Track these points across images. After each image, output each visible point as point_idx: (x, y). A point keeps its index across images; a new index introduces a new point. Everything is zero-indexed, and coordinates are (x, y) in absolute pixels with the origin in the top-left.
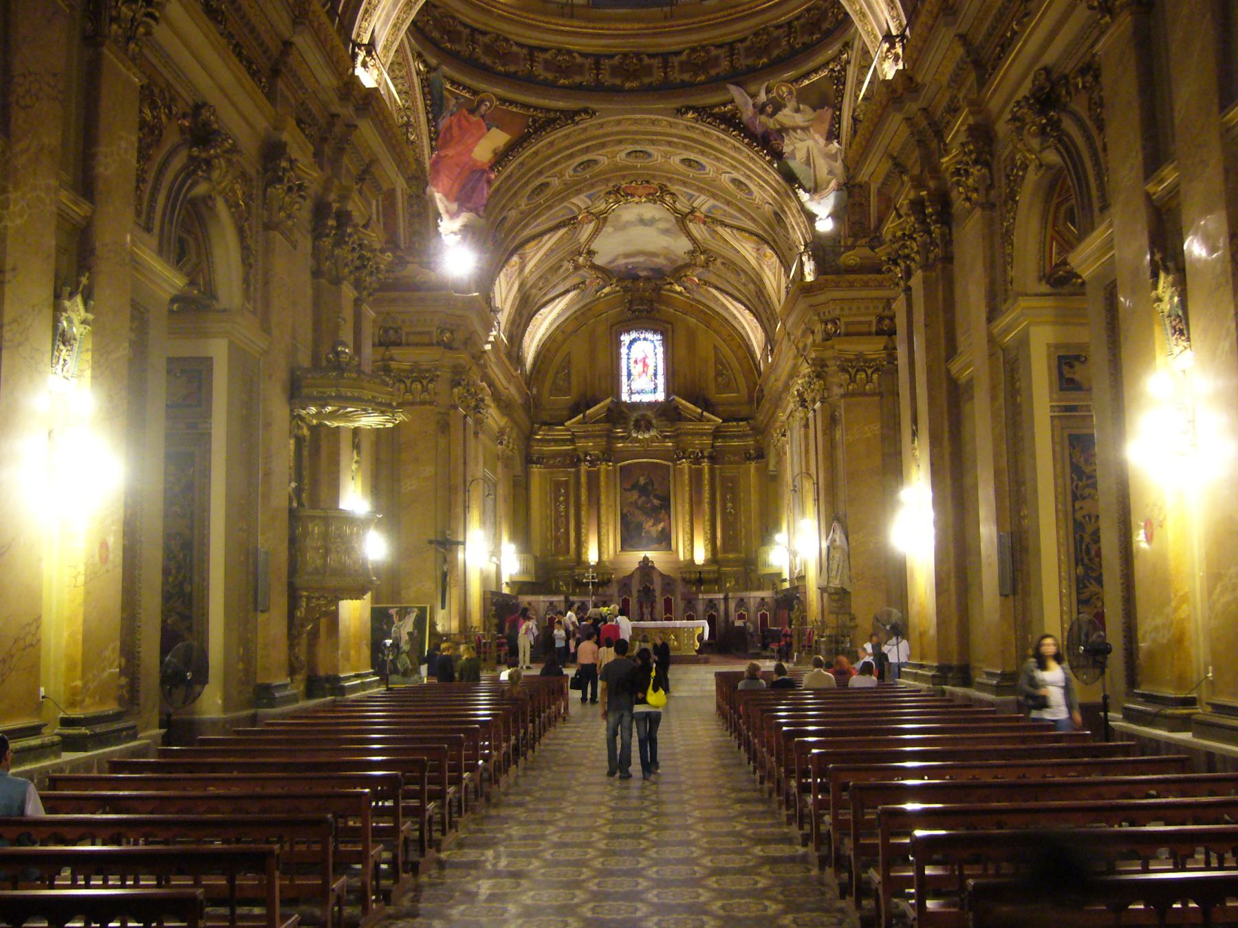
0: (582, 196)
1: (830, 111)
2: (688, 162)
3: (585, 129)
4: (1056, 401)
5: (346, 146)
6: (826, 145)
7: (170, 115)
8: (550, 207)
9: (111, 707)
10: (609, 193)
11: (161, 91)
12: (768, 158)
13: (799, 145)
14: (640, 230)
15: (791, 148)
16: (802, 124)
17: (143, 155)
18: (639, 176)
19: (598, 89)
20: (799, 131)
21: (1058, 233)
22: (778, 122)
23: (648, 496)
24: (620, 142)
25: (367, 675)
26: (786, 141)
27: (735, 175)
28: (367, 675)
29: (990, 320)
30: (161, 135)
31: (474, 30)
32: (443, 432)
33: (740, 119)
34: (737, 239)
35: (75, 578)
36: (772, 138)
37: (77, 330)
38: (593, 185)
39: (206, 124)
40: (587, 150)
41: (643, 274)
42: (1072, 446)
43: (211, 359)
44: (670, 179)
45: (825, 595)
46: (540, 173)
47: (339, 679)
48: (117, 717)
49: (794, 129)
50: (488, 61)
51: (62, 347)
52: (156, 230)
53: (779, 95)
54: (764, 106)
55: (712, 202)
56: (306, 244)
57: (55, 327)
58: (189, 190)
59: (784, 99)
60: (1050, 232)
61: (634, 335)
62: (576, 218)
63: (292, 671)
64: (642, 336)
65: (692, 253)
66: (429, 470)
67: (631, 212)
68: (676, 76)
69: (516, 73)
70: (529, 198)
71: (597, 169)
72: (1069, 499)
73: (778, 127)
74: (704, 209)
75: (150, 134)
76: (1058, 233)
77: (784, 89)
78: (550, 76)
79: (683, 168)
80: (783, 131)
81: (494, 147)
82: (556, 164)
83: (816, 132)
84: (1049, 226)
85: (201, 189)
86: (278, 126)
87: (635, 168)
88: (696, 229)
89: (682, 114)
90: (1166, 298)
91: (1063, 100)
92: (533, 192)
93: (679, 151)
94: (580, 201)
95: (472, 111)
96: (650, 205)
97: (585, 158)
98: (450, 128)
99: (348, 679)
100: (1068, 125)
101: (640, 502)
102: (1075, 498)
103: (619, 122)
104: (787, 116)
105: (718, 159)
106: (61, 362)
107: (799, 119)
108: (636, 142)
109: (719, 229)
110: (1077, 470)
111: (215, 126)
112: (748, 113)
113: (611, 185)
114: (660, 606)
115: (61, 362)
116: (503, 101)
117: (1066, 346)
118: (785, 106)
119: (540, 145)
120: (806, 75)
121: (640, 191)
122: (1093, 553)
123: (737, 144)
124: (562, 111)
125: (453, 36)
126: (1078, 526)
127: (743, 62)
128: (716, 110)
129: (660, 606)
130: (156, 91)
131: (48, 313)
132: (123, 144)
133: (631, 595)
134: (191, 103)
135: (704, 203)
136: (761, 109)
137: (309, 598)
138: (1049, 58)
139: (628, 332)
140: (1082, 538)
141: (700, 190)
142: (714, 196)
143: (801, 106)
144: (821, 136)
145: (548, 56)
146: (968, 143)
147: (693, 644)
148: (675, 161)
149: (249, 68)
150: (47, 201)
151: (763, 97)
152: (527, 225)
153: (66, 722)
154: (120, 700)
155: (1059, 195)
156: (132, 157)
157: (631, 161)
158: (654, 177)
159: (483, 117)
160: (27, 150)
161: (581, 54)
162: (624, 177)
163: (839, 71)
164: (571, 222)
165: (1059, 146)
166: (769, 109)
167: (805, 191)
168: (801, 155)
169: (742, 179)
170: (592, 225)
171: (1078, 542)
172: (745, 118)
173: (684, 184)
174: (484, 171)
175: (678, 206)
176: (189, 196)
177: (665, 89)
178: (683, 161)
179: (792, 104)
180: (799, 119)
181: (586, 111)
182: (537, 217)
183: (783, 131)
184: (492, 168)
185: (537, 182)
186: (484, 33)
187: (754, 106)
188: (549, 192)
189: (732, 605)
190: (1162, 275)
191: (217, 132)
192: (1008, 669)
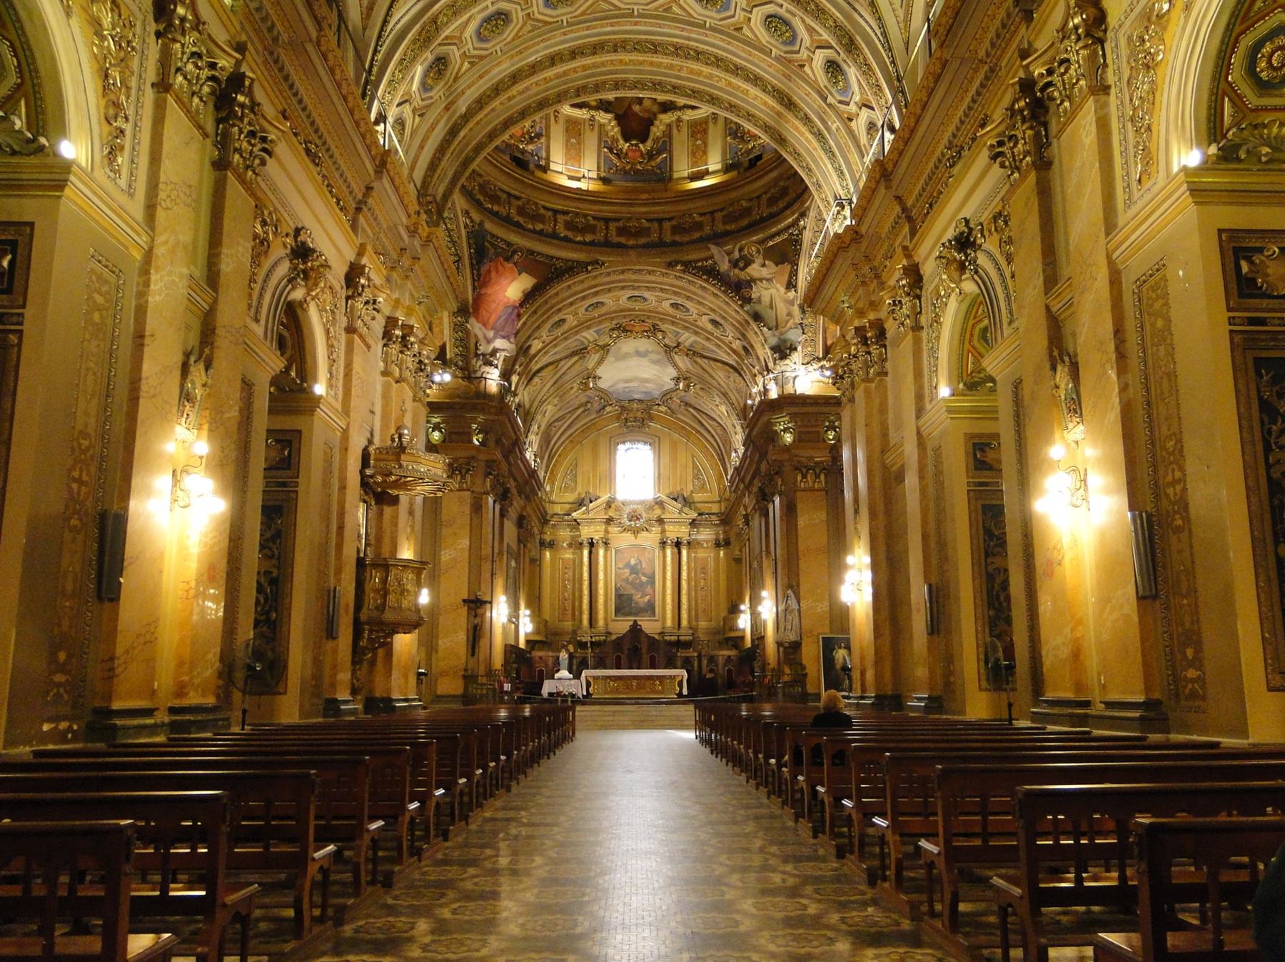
0: (591, 331)
1: (789, 266)
2: (675, 306)
3: (596, 277)
4: (972, 477)
5: (411, 274)
6: (786, 293)
7: (275, 234)
8: (566, 339)
9: (210, 700)
10: (613, 329)
11: (270, 213)
12: (739, 303)
14: (634, 362)
17: (256, 259)
18: (637, 316)
19: (607, 244)
21: (973, 347)
22: (749, 275)
23: (637, 574)
24: (623, 288)
25: (414, 700)
27: (713, 316)
28: (414, 700)
29: (918, 417)
30: (269, 247)
31: (509, 195)
32: (476, 513)
33: (718, 271)
34: (713, 369)
35: (187, 591)
37: (198, 392)
38: (600, 323)
39: (303, 243)
40: (596, 293)
41: (637, 396)
42: (984, 513)
43: (300, 432)
44: (661, 320)
45: (781, 649)
46: (560, 310)
47: (391, 700)
48: (214, 709)
49: (761, 280)
50: (521, 220)
51: (186, 403)
52: (263, 322)
55: (693, 338)
56: (378, 347)
57: (182, 386)
58: (289, 293)
60: (967, 346)
61: (628, 445)
62: (586, 348)
63: (354, 692)
64: (635, 446)
65: (677, 380)
66: (465, 543)
67: (628, 345)
68: (668, 238)
69: (542, 230)
70: (549, 331)
71: (603, 310)
72: (983, 556)
74: (687, 344)
75: (261, 246)
76: (973, 347)
78: (570, 234)
79: (671, 311)
80: (750, 282)
81: (523, 288)
82: (571, 304)
84: (967, 342)
85: (298, 294)
86: (360, 254)
87: (634, 310)
88: (683, 362)
89: (673, 266)
90: (1063, 386)
91: (979, 242)
92: (552, 326)
93: (668, 296)
94: (589, 335)
95: (507, 259)
96: (643, 339)
97: (595, 300)
98: (489, 271)
99: (399, 700)
100: (982, 260)
101: (630, 579)
102: (987, 555)
103: (623, 272)
104: (755, 270)
105: (700, 303)
106: (185, 416)
107: (764, 272)
108: (634, 288)
109: (698, 360)
110: (989, 533)
111: (311, 245)
112: (724, 266)
113: (614, 322)
114: (646, 658)
115: (185, 416)
116: (532, 252)
117: (980, 436)
118: (754, 262)
119: (559, 288)
120: (773, 236)
121: (637, 329)
122: (1002, 598)
123: (716, 292)
124: (578, 262)
125: (494, 199)
126: (990, 577)
127: (720, 227)
128: (700, 264)
129: (646, 658)
130: (266, 213)
131: (177, 373)
132: (241, 249)
133: (622, 653)
134: (293, 227)
135: (687, 338)
136: (735, 264)
137: (371, 632)
138: (966, 212)
139: (624, 443)
140: (993, 587)
141: (686, 328)
142: (696, 333)
144: (781, 283)
145: (568, 218)
146: (901, 279)
147: (675, 689)
148: (666, 304)
149: (338, 203)
150: (180, 285)
151: (736, 255)
152: (546, 353)
153: (173, 711)
154: (218, 697)
155: (975, 318)
156: (247, 260)
157: (630, 305)
158: (649, 317)
159: (515, 264)
160: (166, 243)
161: (594, 218)
162: (625, 317)
163: (797, 235)
164: (581, 352)
165: (975, 276)
166: (741, 264)
167: (770, 329)
168: (766, 300)
169: (718, 319)
170: (597, 356)
171: (990, 590)
172: (722, 270)
173: (673, 323)
174: (516, 307)
175: (667, 341)
176: (289, 299)
177: (659, 246)
178: (672, 305)
179: (759, 260)
180: (764, 272)
181: (596, 262)
182: (556, 346)
183: (750, 282)
184: (522, 305)
185: (556, 318)
186: (518, 198)
187: (730, 261)
188: (566, 327)
189: (705, 662)
190: (1059, 368)
191: (313, 251)
192: (935, 694)
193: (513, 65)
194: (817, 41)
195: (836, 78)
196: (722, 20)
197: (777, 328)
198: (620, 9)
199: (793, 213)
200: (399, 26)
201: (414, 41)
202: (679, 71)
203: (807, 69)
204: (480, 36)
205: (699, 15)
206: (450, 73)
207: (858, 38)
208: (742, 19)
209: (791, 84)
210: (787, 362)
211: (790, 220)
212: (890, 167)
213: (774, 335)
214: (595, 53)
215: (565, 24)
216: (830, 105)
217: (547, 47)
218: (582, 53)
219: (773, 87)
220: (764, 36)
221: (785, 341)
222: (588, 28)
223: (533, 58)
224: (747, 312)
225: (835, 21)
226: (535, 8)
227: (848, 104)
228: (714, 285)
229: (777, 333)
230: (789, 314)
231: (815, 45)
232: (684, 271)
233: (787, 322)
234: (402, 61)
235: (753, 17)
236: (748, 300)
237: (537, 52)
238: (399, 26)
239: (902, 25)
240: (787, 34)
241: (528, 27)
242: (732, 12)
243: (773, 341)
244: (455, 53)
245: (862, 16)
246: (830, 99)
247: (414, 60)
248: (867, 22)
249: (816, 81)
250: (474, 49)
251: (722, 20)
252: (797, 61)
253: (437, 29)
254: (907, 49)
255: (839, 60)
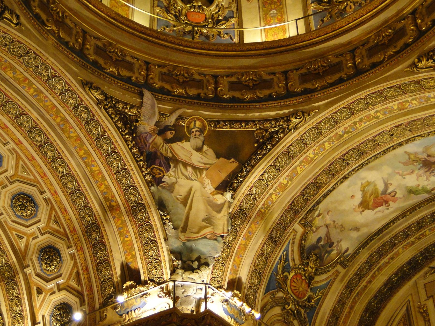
6: (213, 194)
12: (148, 178)
13: (182, 181)
15: (174, 180)
16: (196, 164)
20: (189, 169)
22: (172, 151)
26: (171, 172)
36: (157, 162)
49: (186, 165)
53: (188, 127)
54: (167, 128)
59: (190, 132)
73: (170, 155)
77: (198, 124)
83: (207, 176)
118: (188, 140)
120: (232, 122)
143: (205, 148)
144: (212, 182)
166: (169, 135)
179: (197, 141)
197: (184, 229)
199: (286, 107)
210: (194, 276)
211: (273, 113)
213: (178, 238)
221: (191, 250)
224: (153, 195)
228: (126, 141)
229: (182, 237)
230: (208, 221)
232: (99, 103)
233: (201, 228)
236: (158, 181)
243: (176, 244)
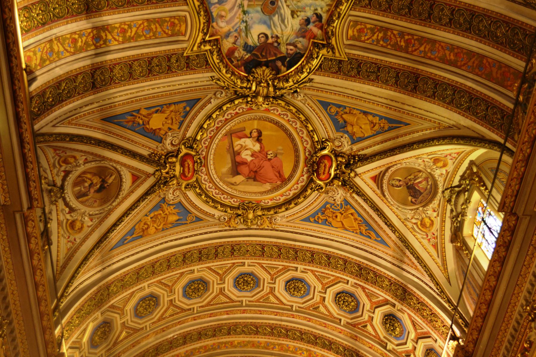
193: (157, 339)
194: (375, 303)
195: (393, 326)
196: (303, 303)
198: (233, 301)
200: (82, 286)
201: (91, 299)
202: (273, 349)
203: (369, 328)
204: (137, 314)
205: (288, 301)
206: (113, 337)
207: (409, 286)
208: (318, 299)
209: (357, 343)
212: (470, 349)
214: (214, 336)
215: (195, 312)
216: (389, 351)
217: (181, 329)
218: (206, 335)
219: (344, 348)
220: (334, 309)
222: (211, 315)
223: (171, 335)
225: (390, 280)
226: (176, 296)
227: (406, 343)
231: (374, 306)
234: (79, 310)
235: (327, 296)
237: (175, 331)
238: (82, 286)
239: (442, 268)
240: (353, 304)
241: (170, 312)
242: (311, 296)
244: (118, 321)
245: (409, 273)
246: (390, 346)
247: (89, 314)
248: (414, 275)
249: (377, 336)
250: (132, 321)
251: (303, 303)
252: (360, 324)
253: (108, 294)
254: (449, 282)
255: (394, 311)
